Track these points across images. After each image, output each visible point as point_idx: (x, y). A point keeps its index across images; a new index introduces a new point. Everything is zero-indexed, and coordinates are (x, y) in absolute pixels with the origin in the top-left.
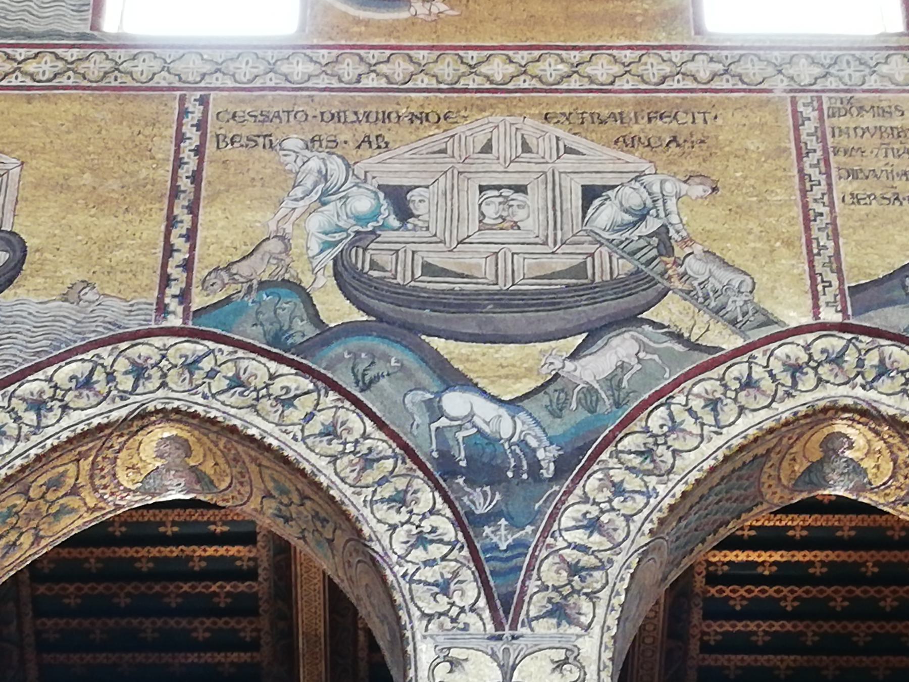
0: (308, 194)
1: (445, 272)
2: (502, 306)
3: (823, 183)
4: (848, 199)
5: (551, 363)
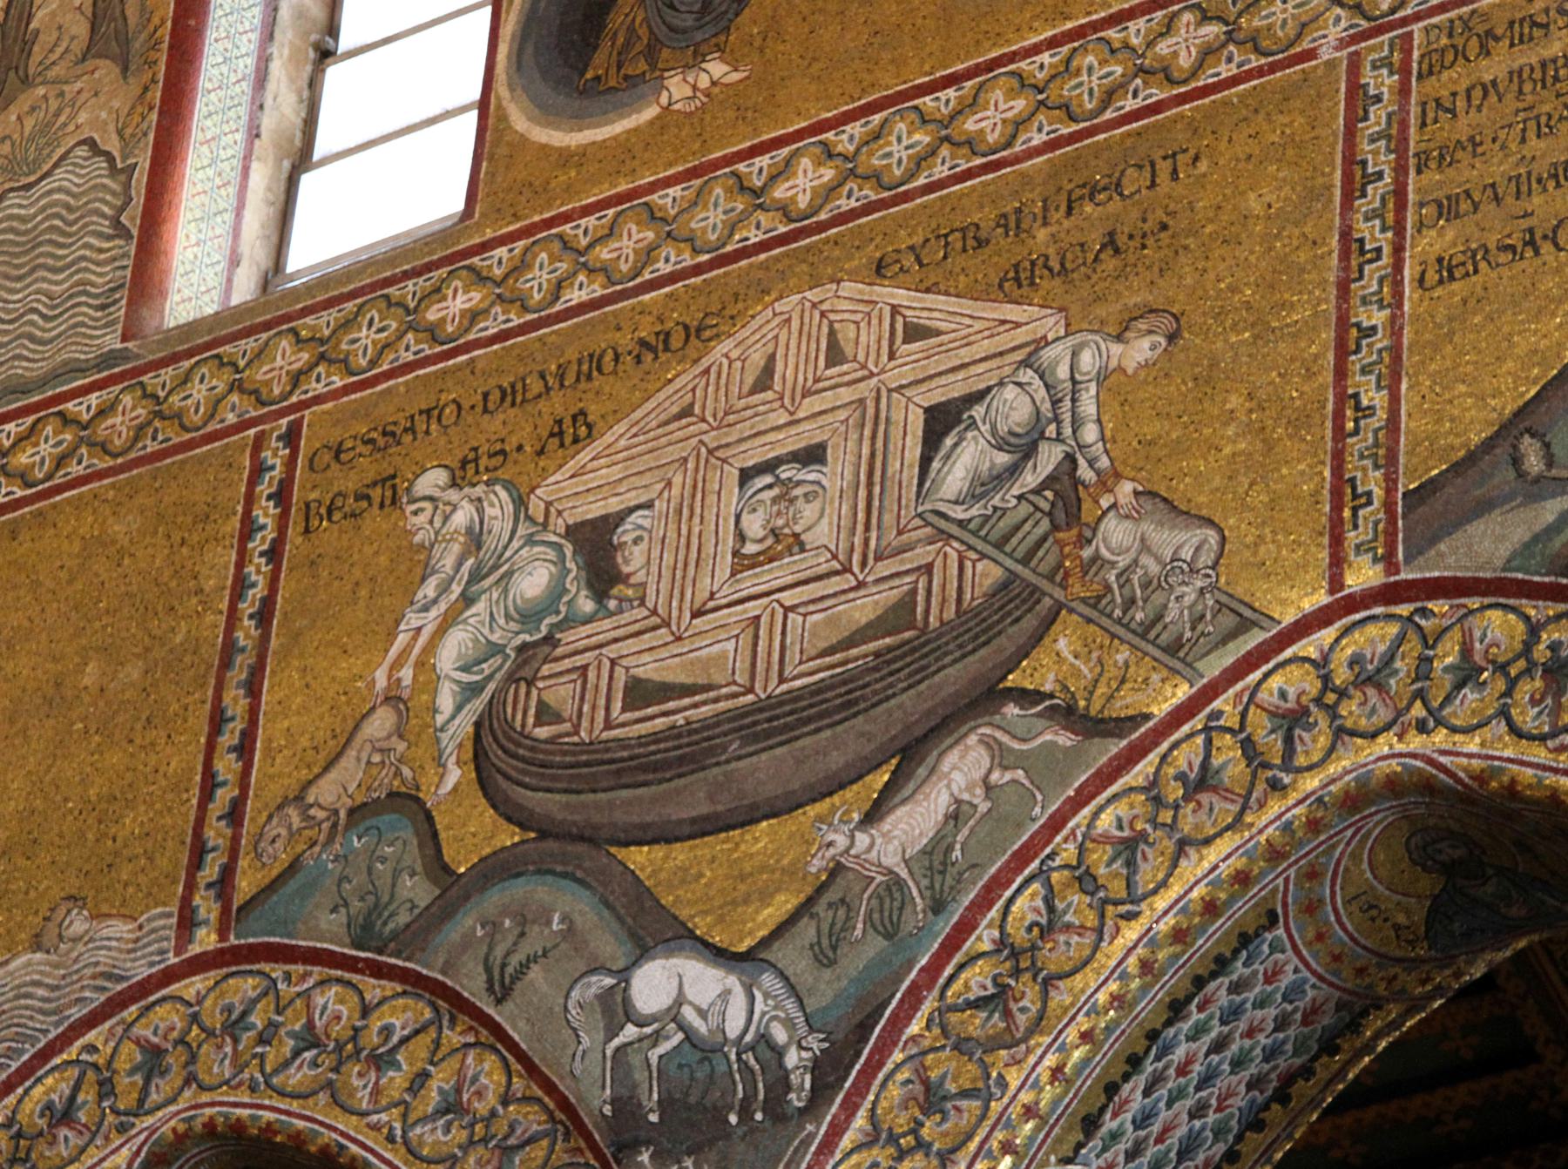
0: (444, 589)
1: (667, 691)
2: (756, 738)
3: (1386, 250)
4: (1432, 277)
5: (830, 844)
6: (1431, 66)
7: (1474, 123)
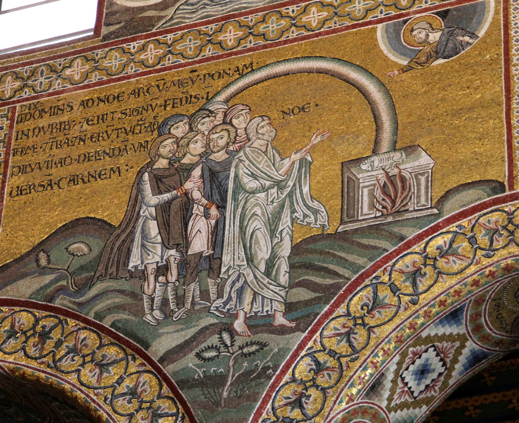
4: (14, 193)
6: (21, 119)
7: (34, 141)
